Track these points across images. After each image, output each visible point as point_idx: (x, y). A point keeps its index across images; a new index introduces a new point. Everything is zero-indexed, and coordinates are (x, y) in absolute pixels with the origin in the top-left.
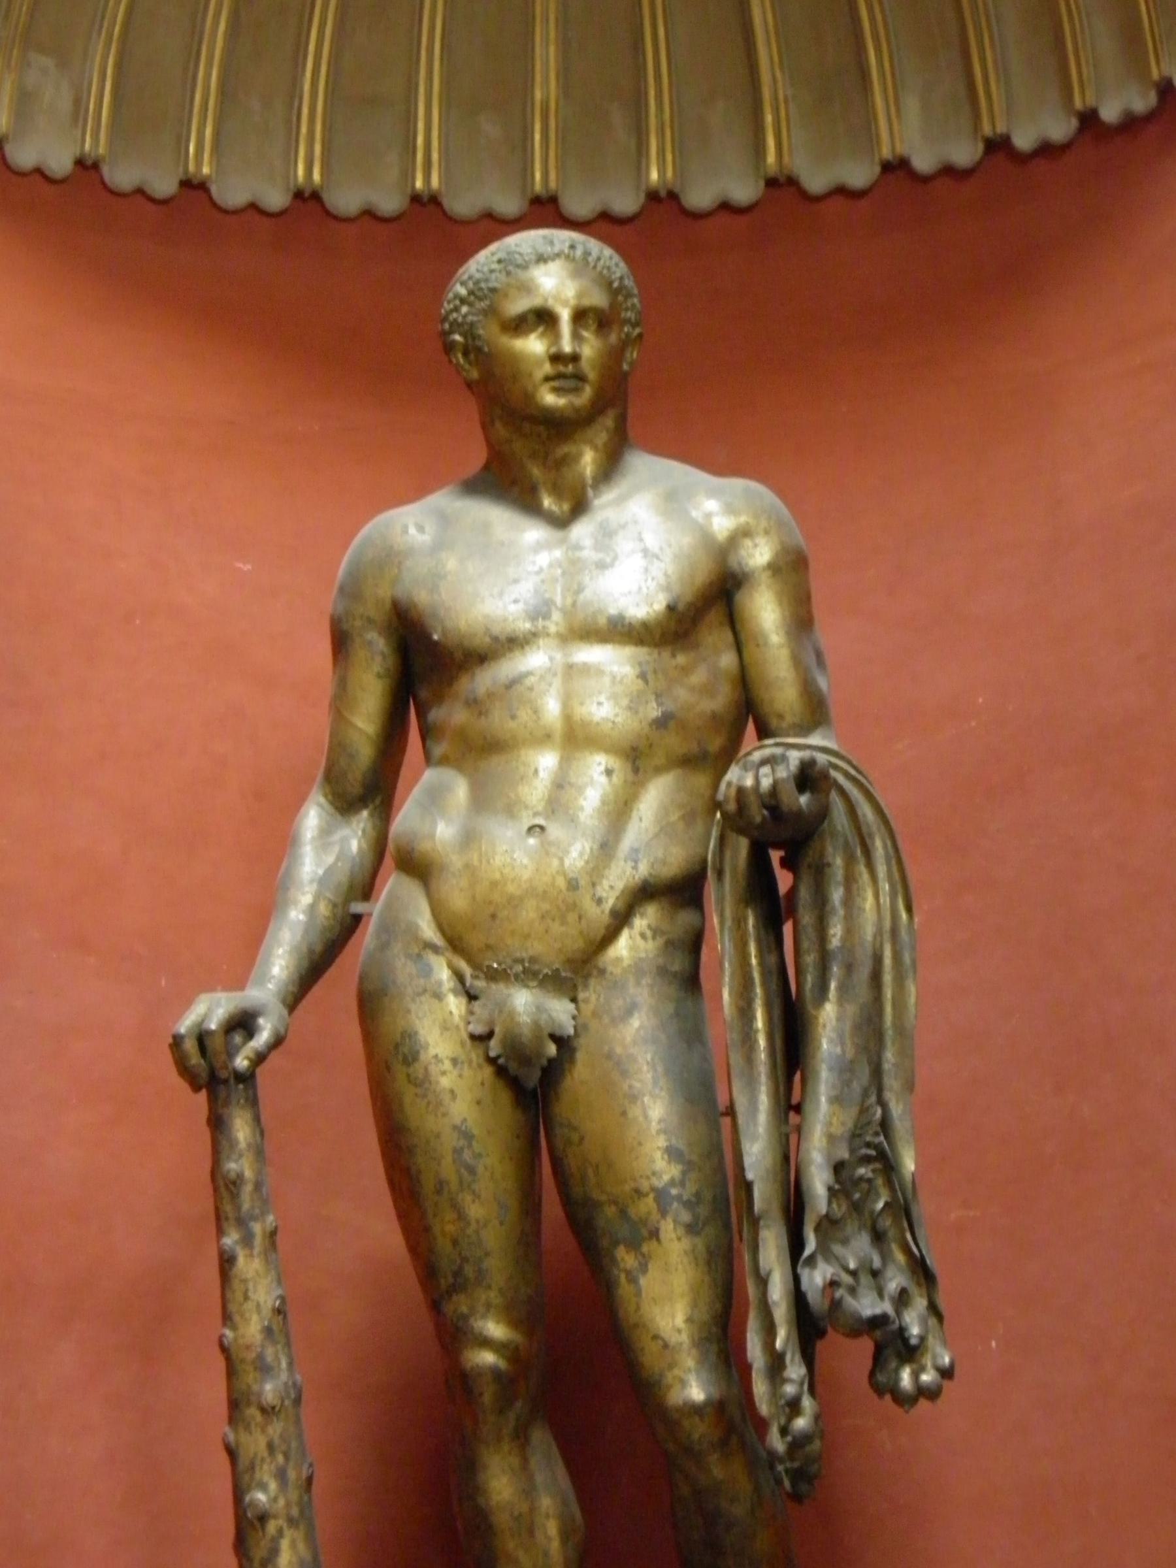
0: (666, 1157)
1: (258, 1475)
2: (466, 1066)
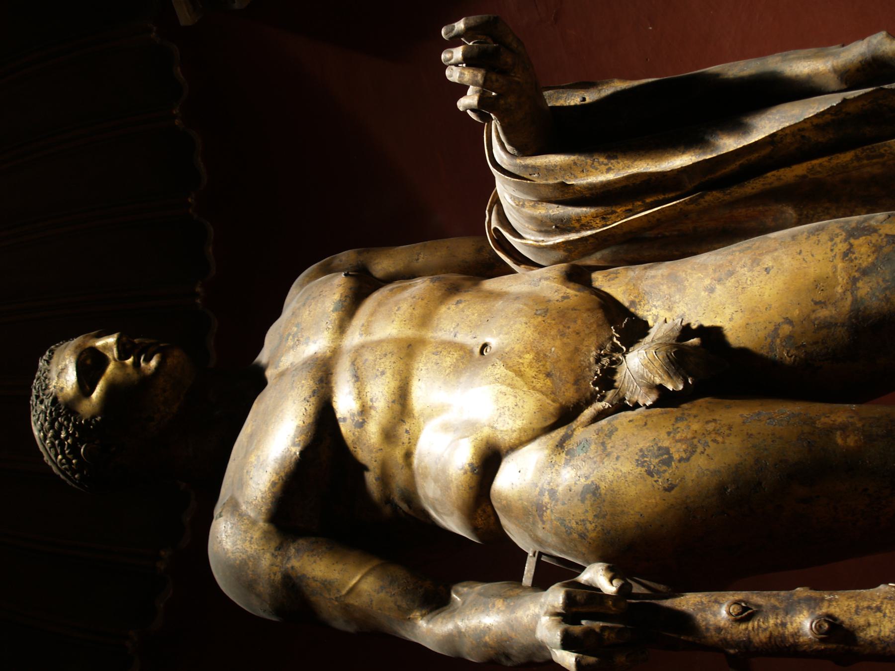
2: (686, 412)
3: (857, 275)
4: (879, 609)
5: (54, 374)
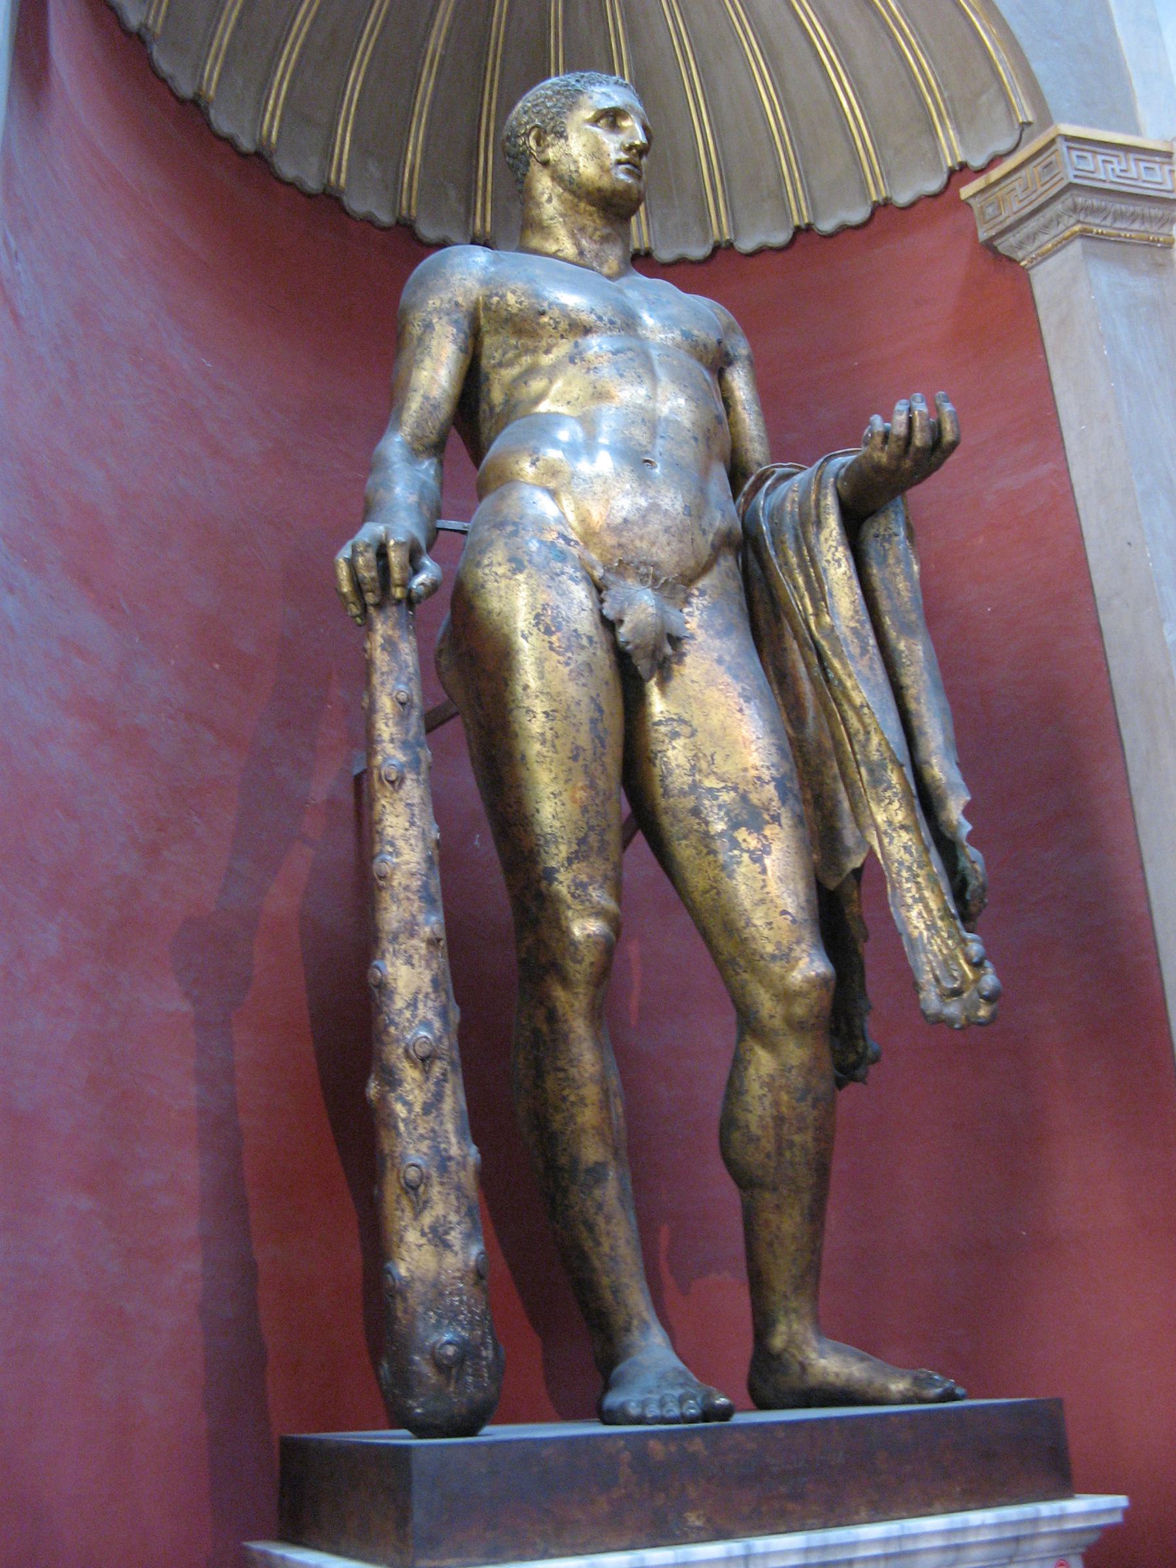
1: (422, 1010)
2: (598, 645)
3: (741, 791)
5: (604, 89)
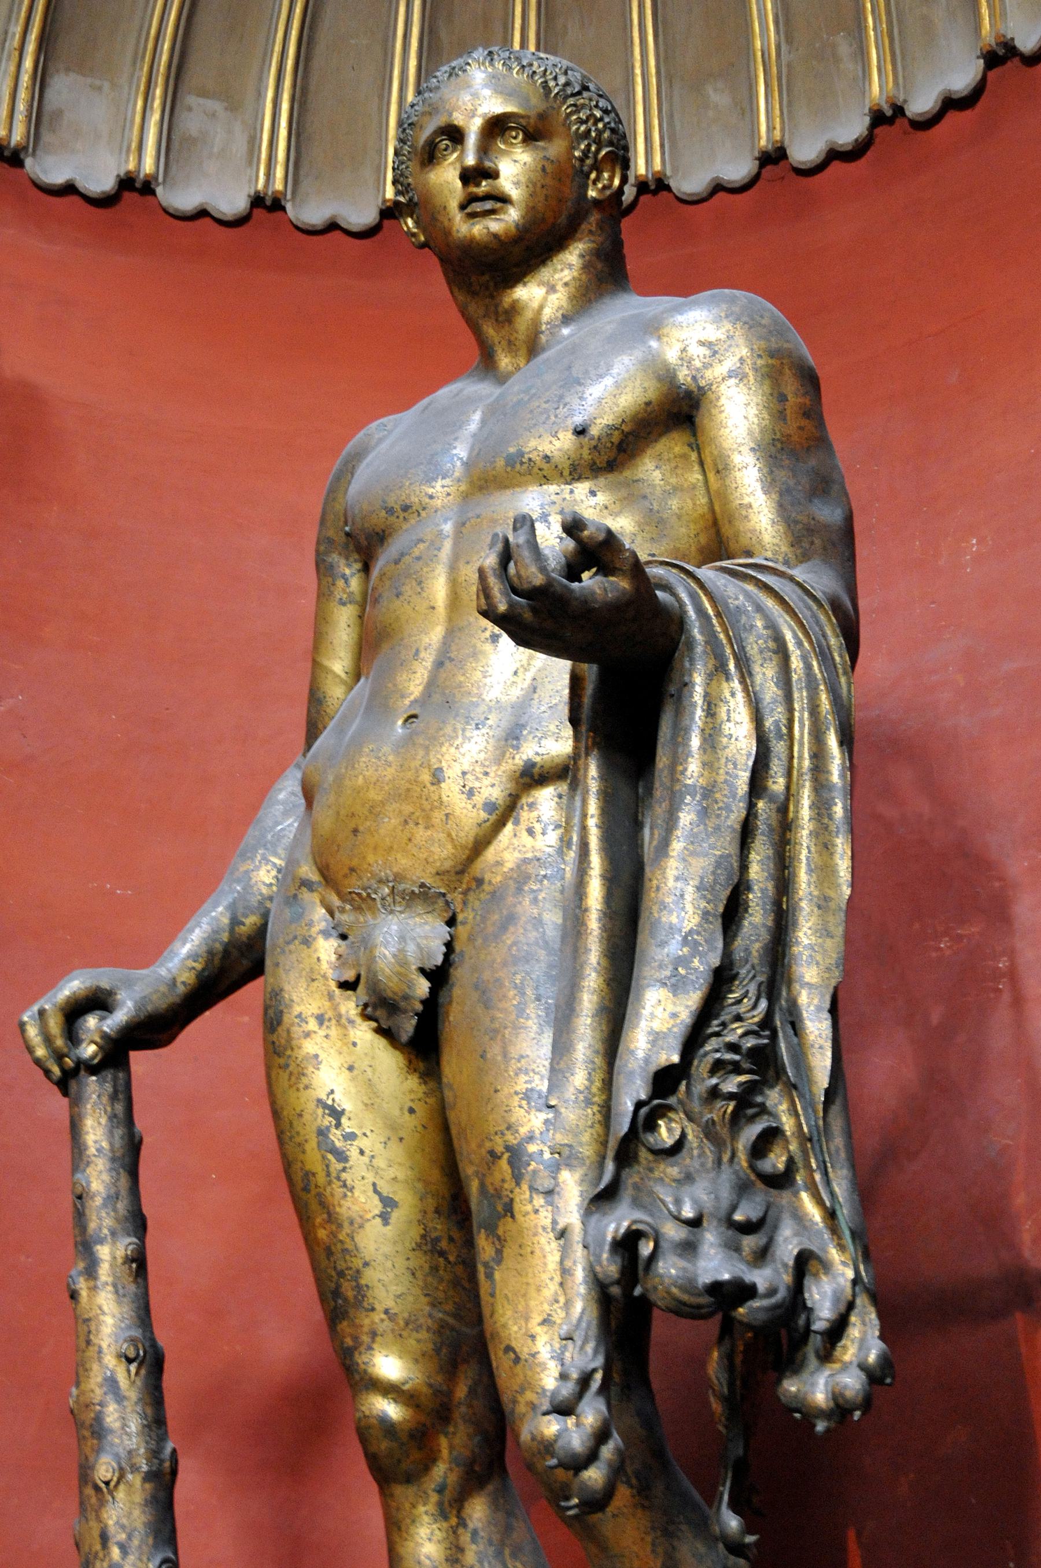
0: (524, 1103)
2: (334, 1022)
4: (88, 1342)
